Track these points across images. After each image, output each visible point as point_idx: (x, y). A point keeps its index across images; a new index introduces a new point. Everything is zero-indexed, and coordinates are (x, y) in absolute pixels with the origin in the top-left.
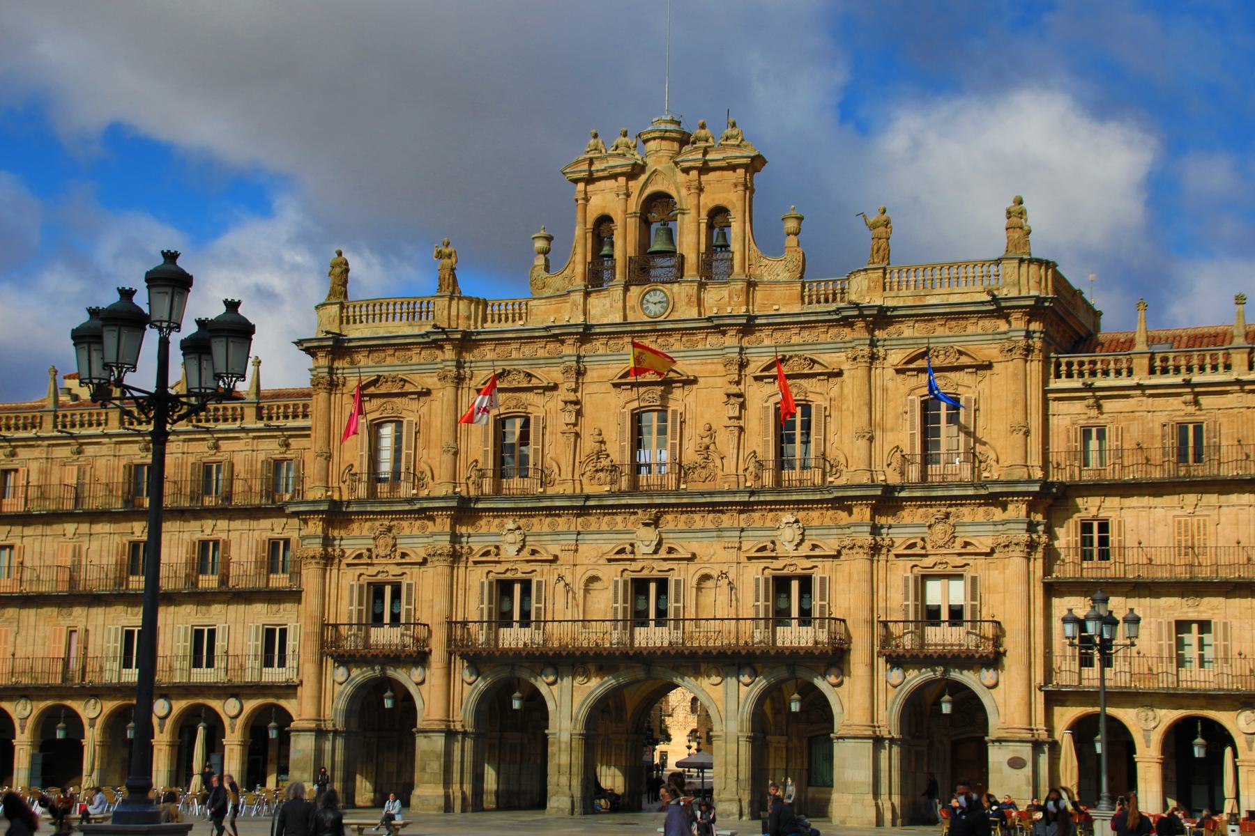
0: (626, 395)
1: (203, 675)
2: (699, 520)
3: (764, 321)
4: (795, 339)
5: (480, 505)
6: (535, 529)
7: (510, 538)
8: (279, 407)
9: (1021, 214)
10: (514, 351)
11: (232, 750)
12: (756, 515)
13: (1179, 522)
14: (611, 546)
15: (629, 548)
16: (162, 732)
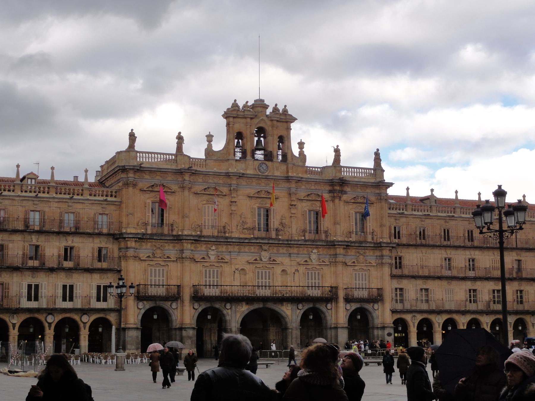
0: (253, 201)
1: (68, 305)
2: (283, 250)
3: (305, 180)
4: (313, 187)
5: (202, 239)
6: (220, 250)
7: (212, 253)
8: (99, 191)
9: (379, 154)
10: (211, 181)
11: (85, 337)
12: (301, 249)
13: (421, 258)
14: (251, 258)
15: (258, 259)
16: (50, 329)
